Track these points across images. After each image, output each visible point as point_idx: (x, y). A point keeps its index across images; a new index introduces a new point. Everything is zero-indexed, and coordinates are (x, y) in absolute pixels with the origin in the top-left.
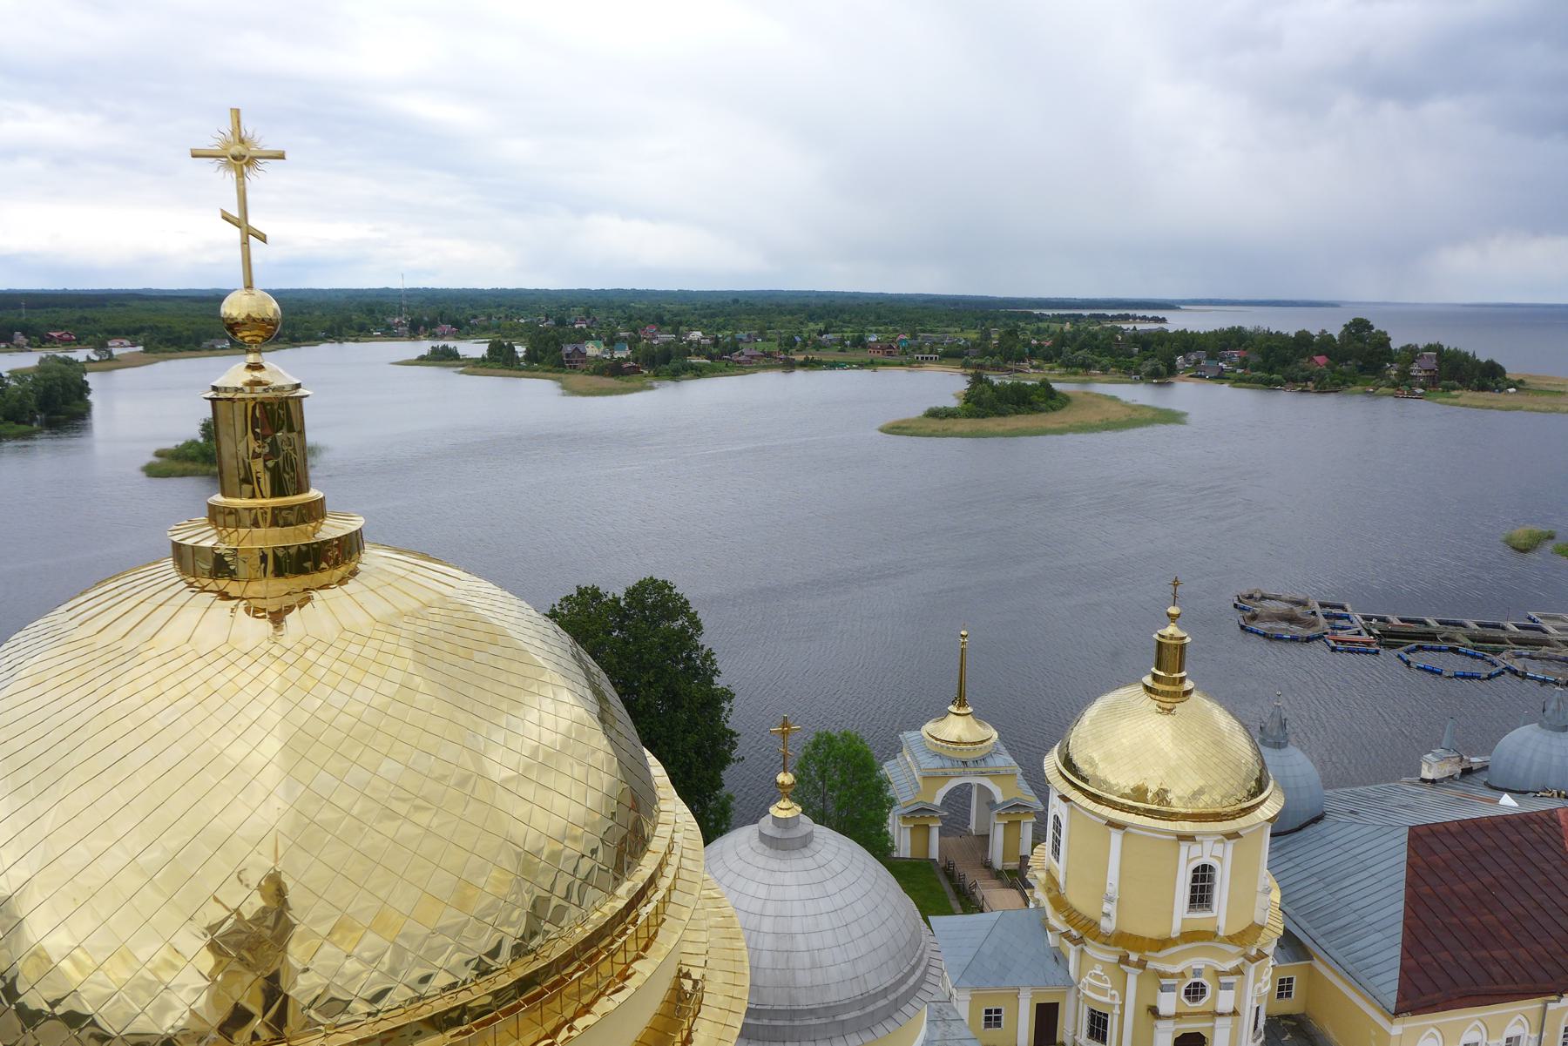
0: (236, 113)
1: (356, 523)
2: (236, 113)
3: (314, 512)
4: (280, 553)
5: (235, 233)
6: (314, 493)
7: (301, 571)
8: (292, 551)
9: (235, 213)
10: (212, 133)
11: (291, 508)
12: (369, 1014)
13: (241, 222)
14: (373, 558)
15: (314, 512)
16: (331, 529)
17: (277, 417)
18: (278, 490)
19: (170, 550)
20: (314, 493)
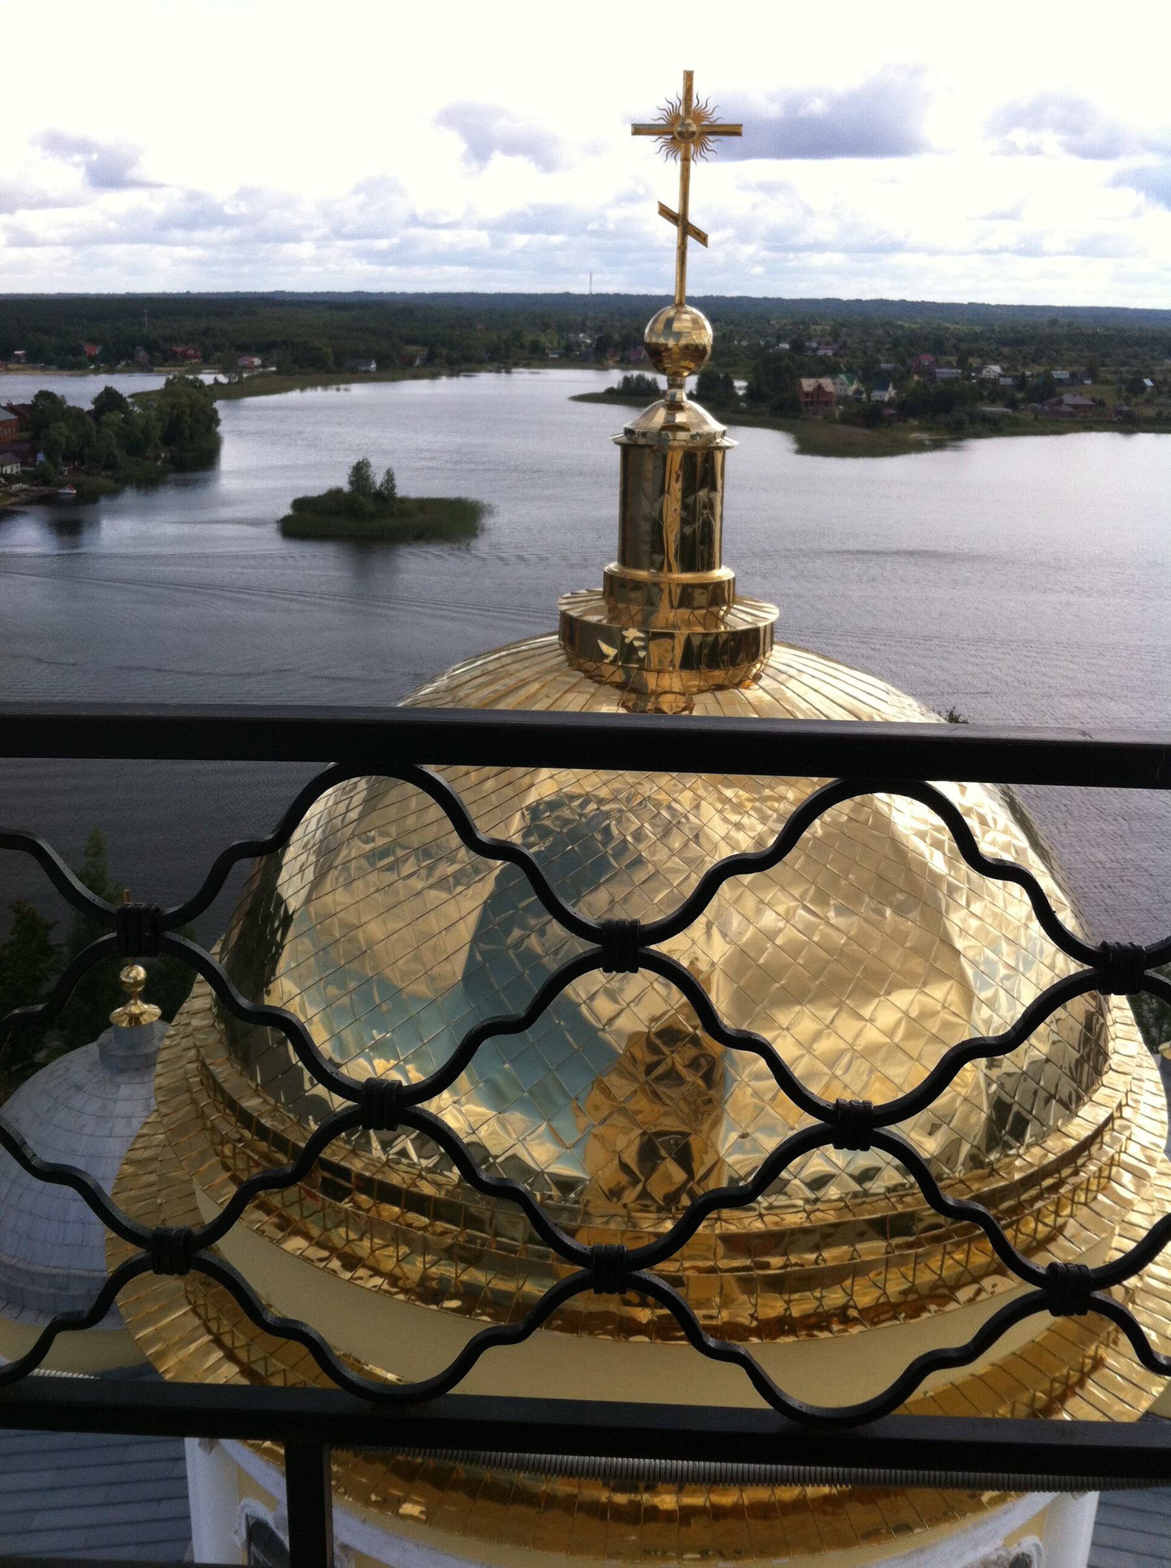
0: (689, 76)
1: (770, 614)
2: (689, 76)
3: (719, 595)
4: (696, 642)
5: (672, 231)
6: (723, 573)
7: (713, 664)
8: (710, 639)
9: (675, 208)
10: (657, 99)
11: (704, 586)
12: (807, 1201)
13: (680, 219)
14: (779, 656)
15: (719, 595)
16: (739, 618)
17: (702, 468)
18: (688, 567)
19: (556, 625)
20: (723, 573)
